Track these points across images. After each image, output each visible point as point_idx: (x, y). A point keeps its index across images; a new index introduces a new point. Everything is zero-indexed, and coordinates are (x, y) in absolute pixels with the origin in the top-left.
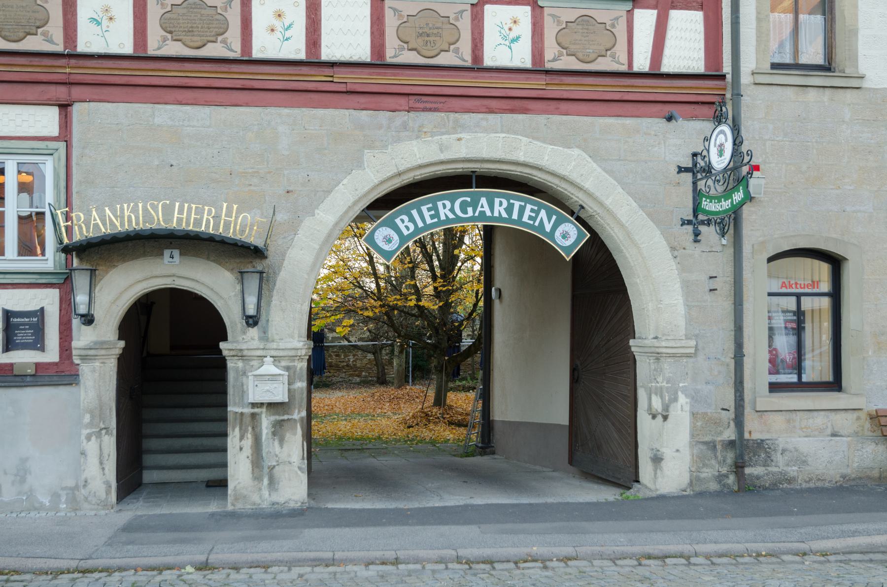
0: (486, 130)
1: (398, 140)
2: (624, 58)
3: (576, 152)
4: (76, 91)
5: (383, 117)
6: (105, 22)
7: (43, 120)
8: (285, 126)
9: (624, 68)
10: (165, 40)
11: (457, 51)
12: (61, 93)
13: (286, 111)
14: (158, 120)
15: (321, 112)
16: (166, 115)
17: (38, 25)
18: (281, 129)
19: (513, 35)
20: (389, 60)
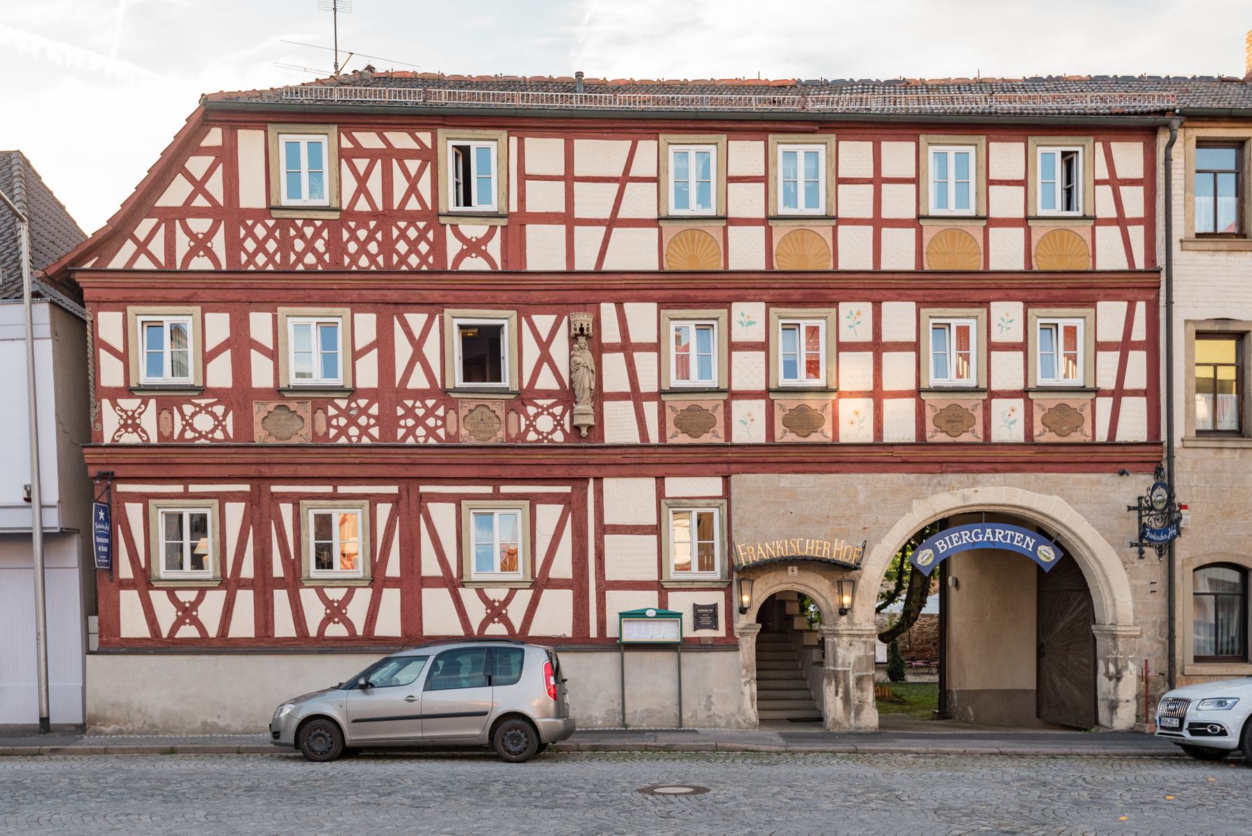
0: (994, 485)
1: (935, 493)
2: (1089, 432)
3: (1056, 498)
4: (733, 467)
5: (925, 478)
6: (749, 422)
7: (714, 486)
8: (861, 484)
9: (1089, 440)
10: (785, 432)
11: (973, 431)
12: (724, 468)
13: (862, 476)
14: (782, 484)
15: (885, 476)
16: (787, 481)
17: (709, 424)
18: (859, 487)
19: (1011, 419)
20: (929, 440)
